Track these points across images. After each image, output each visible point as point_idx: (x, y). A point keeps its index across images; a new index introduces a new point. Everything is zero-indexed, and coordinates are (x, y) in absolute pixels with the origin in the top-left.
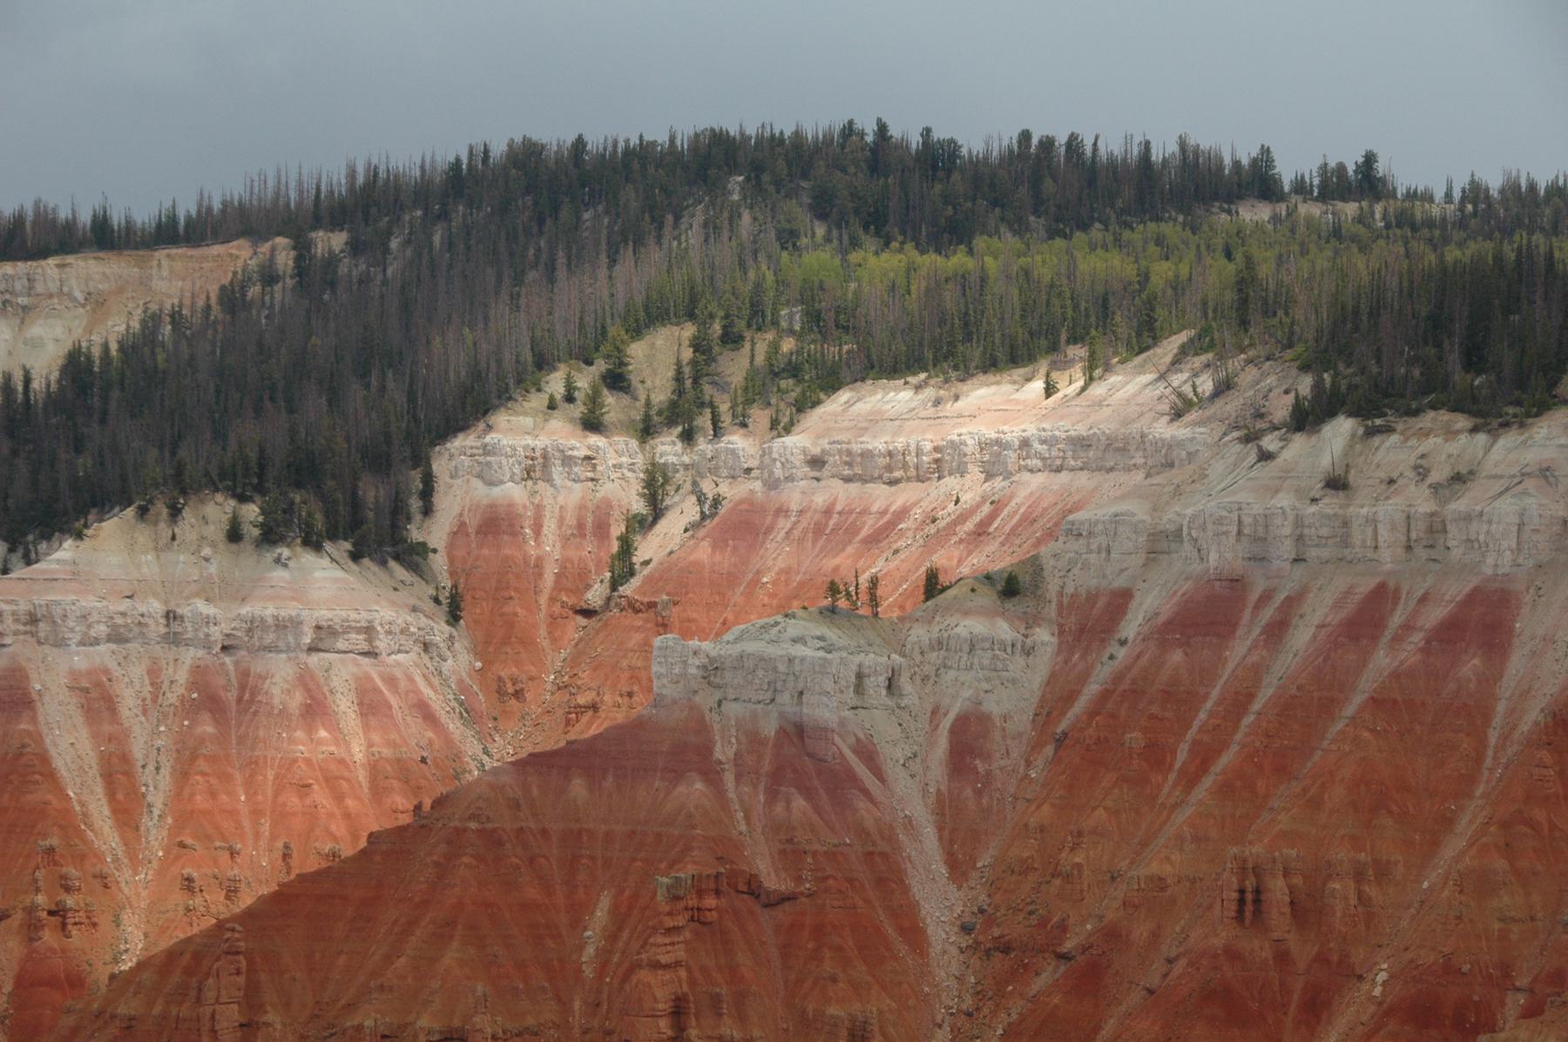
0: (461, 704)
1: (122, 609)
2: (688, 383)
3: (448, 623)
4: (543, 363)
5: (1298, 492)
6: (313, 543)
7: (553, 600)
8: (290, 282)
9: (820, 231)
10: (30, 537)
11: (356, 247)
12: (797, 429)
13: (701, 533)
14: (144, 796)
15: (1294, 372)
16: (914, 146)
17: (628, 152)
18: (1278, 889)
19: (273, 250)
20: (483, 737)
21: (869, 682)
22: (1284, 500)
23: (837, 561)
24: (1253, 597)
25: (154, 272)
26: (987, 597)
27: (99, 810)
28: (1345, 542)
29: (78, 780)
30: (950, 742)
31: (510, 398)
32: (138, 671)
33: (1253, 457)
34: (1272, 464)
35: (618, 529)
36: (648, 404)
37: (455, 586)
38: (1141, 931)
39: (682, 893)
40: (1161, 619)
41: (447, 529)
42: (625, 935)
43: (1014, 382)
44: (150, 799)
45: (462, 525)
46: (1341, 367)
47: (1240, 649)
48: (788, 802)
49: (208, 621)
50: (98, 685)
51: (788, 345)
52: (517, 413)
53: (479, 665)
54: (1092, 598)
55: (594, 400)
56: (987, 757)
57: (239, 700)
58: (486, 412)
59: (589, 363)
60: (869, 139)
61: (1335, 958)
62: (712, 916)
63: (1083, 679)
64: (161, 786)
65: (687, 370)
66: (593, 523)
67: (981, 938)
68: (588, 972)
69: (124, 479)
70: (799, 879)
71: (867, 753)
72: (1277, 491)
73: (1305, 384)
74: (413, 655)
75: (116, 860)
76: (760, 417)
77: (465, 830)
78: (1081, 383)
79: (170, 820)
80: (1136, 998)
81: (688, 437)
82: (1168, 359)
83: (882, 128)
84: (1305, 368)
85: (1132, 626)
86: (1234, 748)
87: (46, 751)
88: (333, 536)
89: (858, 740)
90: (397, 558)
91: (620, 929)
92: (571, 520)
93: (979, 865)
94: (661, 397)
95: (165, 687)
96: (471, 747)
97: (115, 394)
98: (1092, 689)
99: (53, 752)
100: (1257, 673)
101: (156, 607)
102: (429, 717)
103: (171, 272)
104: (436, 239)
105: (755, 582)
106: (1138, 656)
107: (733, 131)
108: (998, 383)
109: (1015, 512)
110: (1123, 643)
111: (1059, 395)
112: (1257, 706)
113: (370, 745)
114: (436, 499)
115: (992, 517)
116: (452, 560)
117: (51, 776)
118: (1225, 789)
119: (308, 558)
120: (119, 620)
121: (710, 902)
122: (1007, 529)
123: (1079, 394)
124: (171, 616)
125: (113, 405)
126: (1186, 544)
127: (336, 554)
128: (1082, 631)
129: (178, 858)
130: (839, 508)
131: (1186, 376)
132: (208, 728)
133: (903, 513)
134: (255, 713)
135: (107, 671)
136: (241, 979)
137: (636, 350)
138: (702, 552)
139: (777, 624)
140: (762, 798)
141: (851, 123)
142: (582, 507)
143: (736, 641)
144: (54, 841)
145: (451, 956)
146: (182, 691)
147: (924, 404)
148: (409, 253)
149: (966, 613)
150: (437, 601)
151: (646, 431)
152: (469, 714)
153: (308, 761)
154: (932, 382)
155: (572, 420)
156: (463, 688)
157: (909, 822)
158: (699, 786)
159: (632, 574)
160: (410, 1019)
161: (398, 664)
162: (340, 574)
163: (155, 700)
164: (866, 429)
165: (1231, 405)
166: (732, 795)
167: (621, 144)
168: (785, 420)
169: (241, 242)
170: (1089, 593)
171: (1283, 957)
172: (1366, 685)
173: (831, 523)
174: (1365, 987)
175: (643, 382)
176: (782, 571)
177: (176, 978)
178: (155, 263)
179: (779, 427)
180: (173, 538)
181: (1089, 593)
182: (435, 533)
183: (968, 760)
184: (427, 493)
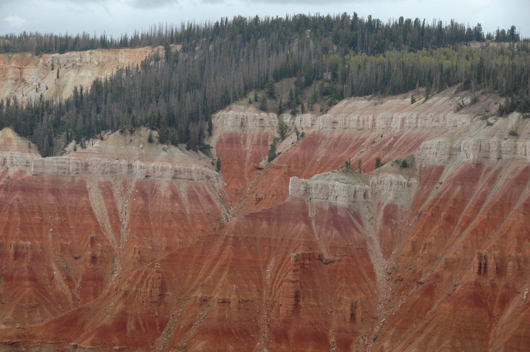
0: (220, 197)
1: (115, 163)
2: (294, 96)
3: (217, 171)
4: (247, 89)
5: (501, 137)
6: (175, 144)
7: (249, 164)
8: (163, 60)
9: (335, 48)
10: (83, 139)
11: (184, 50)
12: (329, 112)
13: (298, 144)
14: (121, 222)
15: (498, 97)
16: (365, 21)
17: (273, 21)
18: (491, 263)
19: (158, 50)
20: (227, 208)
21: (358, 194)
22: (495, 139)
23: (342, 155)
24: (485, 170)
25: (120, 55)
26: (396, 168)
27: (108, 226)
28: (515, 153)
29: (101, 216)
30: (384, 214)
31: (237, 100)
32: (119, 183)
33: (485, 124)
34: (492, 127)
35: (270, 143)
36: (281, 102)
37: (219, 159)
38: (446, 275)
39: (299, 259)
40: (454, 176)
41: (216, 141)
42: (280, 271)
43: (400, 99)
44: (123, 223)
45: (221, 140)
46: (514, 95)
47: (481, 186)
48: (332, 231)
49: (141, 167)
50: (108, 186)
51: (326, 85)
52: (239, 105)
53: (226, 184)
54: (431, 169)
55: (264, 101)
56: (396, 219)
57: (151, 193)
58: (229, 104)
59: (262, 88)
60: (351, 18)
61: (511, 286)
62: (308, 266)
63: (428, 194)
64: (127, 219)
65: (294, 92)
66: (262, 141)
67: (393, 276)
68: (269, 283)
69: (112, 122)
70: (335, 256)
71: (357, 216)
72: (493, 136)
73: (503, 101)
74: (205, 181)
75: (113, 242)
76: (317, 106)
77: (230, 236)
78: (424, 99)
79: (129, 230)
80: (445, 296)
81: (294, 114)
82: (453, 92)
83: (355, 15)
84: (502, 96)
85: (444, 178)
86: (477, 218)
87: (91, 207)
88: (181, 142)
89: (354, 212)
90: (200, 150)
91: (278, 269)
92: (255, 139)
93: (393, 253)
94: (284, 101)
95: (128, 188)
96: (223, 211)
97: (109, 95)
98: (431, 198)
99: (93, 207)
100: (485, 195)
101: (124, 162)
102: (210, 201)
103: (125, 56)
104: (211, 47)
105: (316, 160)
106: (446, 188)
107: (307, 15)
108: (395, 99)
109: (402, 141)
110: (441, 183)
111: (416, 103)
112: (485, 205)
113: (192, 209)
114: (212, 132)
115: (394, 142)
116: (217, 151)
117: (93, 215)
118: (475, 231)
119: (173, 148)
120: (114, 167)
121: (307, 262)
122: (399, 146)
123: (423, 102)
124: (130, 166)
125: (108, 99)
126: (462, 152)
127: (182, 148)
128: (427, 179)
129: (132, 242)
130: (342, 138)
131: (459, 97)
132: (141, 201)
133: (364, 140)
134: (156, 197)
135: (110, 182)
136: (160, 280)
137: (277, 85)
138: (297, 150)
139: (329, 174)
140: (324, 229)
141: (345, 13)
142: (259, 135)
143: (316, 179)
144: (93, 235)
145: (225, 275)
146: (133, 189)
147: (371, 105)
148: (202, 52)
149: (390, 173)
150: (213, 164)
151: (280, 112)
152: (223, 200)
153: (172, 213)
154: (374, 98)
155: (256, 107)
156: (221, 192)
157: (370, 239)
158: (303, 225)
159: (275, 157)
160: (213, 295)
161: (201, 183)
162: (183, 154)
163: (125, 192)
164: (352, 113)
165: (477, 108)
166: (314, 228)
167: (271, 19)
168: (325, 109)
169: (148, 47)
170: (430, 167)
171: (494, 286)
172: (522, 199)
173: (340, 143)
174: (520, 296)
175: (279, 96)
176: (323, 157)
177: (139, 280)
178: (120, 53)
179: (323, 111)
180: (131, 141)
181: (430, 167)
182: (213, 142)
183: (390, 219)
184: (211, 129)
